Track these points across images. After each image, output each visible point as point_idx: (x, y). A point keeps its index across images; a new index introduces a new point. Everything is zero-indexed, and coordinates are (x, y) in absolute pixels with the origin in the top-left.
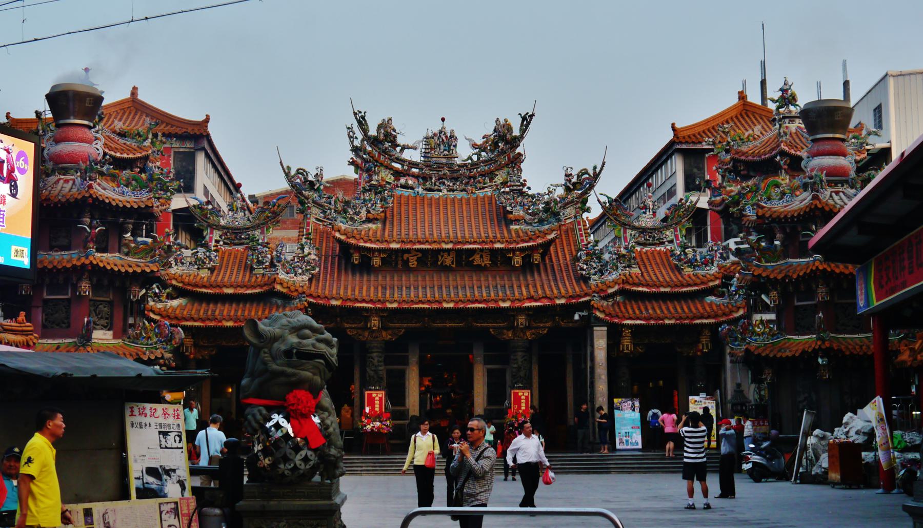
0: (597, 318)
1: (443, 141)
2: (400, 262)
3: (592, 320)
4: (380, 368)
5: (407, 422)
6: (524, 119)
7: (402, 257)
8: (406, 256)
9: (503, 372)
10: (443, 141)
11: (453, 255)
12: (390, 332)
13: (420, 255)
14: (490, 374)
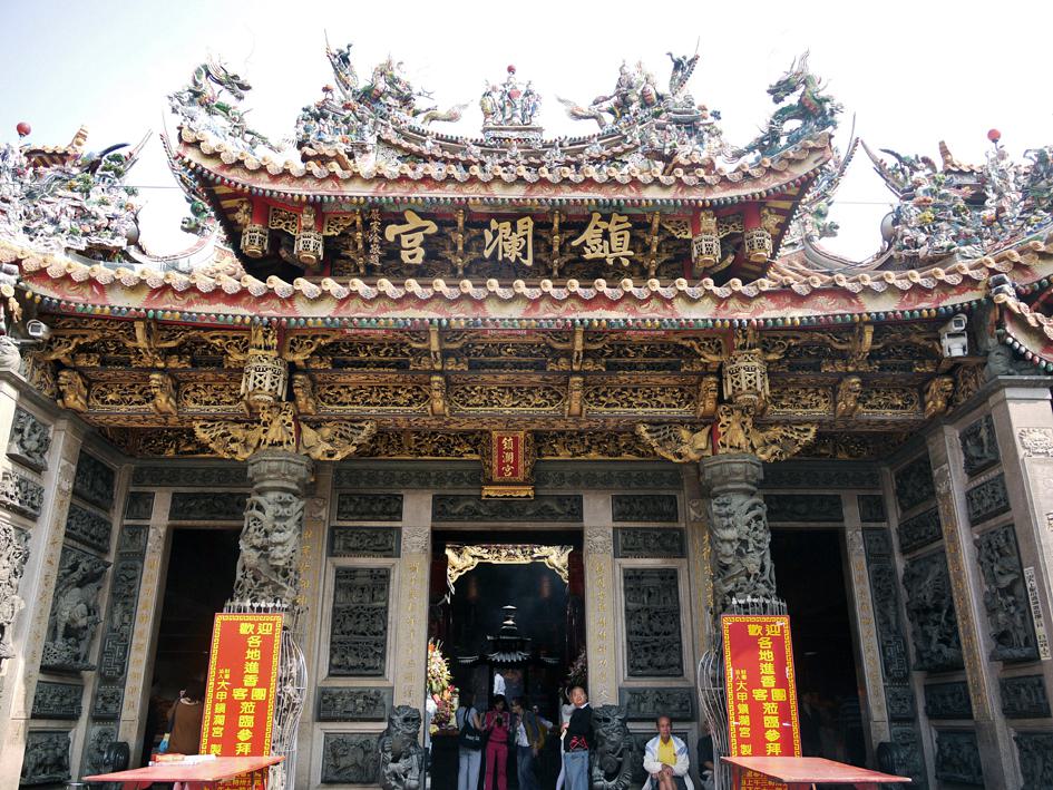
0: (1017, 357)
1: (511, 103)
2: (375, 249)
3: (998, 363)
4: (276, 537)
5: (384, 726)
6: (678, 65)
7: (382, 235)
8: (391, 232)
9: (669, 578)
10: (511, 103)
11: (526, 225)
12: (327, 432)
13: (433, 228)
14: (633, 579)
